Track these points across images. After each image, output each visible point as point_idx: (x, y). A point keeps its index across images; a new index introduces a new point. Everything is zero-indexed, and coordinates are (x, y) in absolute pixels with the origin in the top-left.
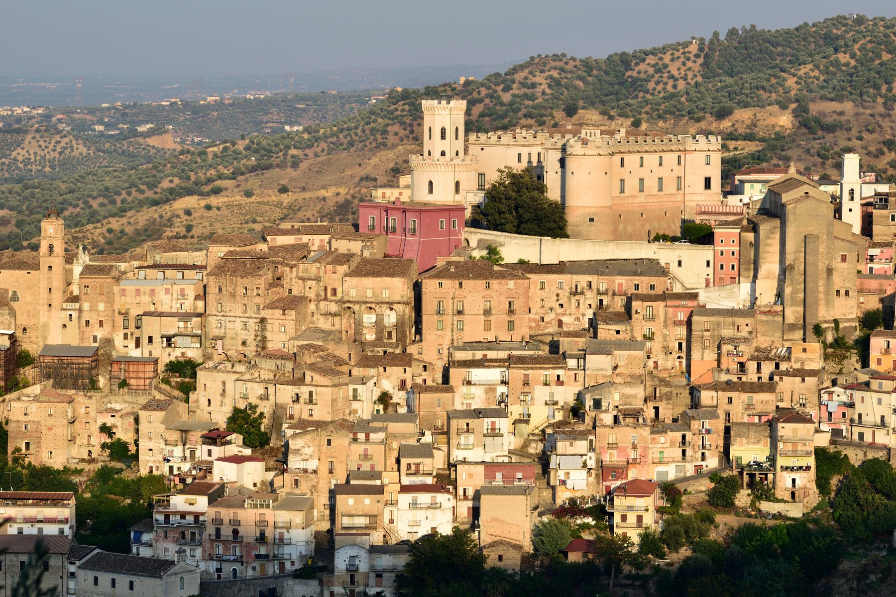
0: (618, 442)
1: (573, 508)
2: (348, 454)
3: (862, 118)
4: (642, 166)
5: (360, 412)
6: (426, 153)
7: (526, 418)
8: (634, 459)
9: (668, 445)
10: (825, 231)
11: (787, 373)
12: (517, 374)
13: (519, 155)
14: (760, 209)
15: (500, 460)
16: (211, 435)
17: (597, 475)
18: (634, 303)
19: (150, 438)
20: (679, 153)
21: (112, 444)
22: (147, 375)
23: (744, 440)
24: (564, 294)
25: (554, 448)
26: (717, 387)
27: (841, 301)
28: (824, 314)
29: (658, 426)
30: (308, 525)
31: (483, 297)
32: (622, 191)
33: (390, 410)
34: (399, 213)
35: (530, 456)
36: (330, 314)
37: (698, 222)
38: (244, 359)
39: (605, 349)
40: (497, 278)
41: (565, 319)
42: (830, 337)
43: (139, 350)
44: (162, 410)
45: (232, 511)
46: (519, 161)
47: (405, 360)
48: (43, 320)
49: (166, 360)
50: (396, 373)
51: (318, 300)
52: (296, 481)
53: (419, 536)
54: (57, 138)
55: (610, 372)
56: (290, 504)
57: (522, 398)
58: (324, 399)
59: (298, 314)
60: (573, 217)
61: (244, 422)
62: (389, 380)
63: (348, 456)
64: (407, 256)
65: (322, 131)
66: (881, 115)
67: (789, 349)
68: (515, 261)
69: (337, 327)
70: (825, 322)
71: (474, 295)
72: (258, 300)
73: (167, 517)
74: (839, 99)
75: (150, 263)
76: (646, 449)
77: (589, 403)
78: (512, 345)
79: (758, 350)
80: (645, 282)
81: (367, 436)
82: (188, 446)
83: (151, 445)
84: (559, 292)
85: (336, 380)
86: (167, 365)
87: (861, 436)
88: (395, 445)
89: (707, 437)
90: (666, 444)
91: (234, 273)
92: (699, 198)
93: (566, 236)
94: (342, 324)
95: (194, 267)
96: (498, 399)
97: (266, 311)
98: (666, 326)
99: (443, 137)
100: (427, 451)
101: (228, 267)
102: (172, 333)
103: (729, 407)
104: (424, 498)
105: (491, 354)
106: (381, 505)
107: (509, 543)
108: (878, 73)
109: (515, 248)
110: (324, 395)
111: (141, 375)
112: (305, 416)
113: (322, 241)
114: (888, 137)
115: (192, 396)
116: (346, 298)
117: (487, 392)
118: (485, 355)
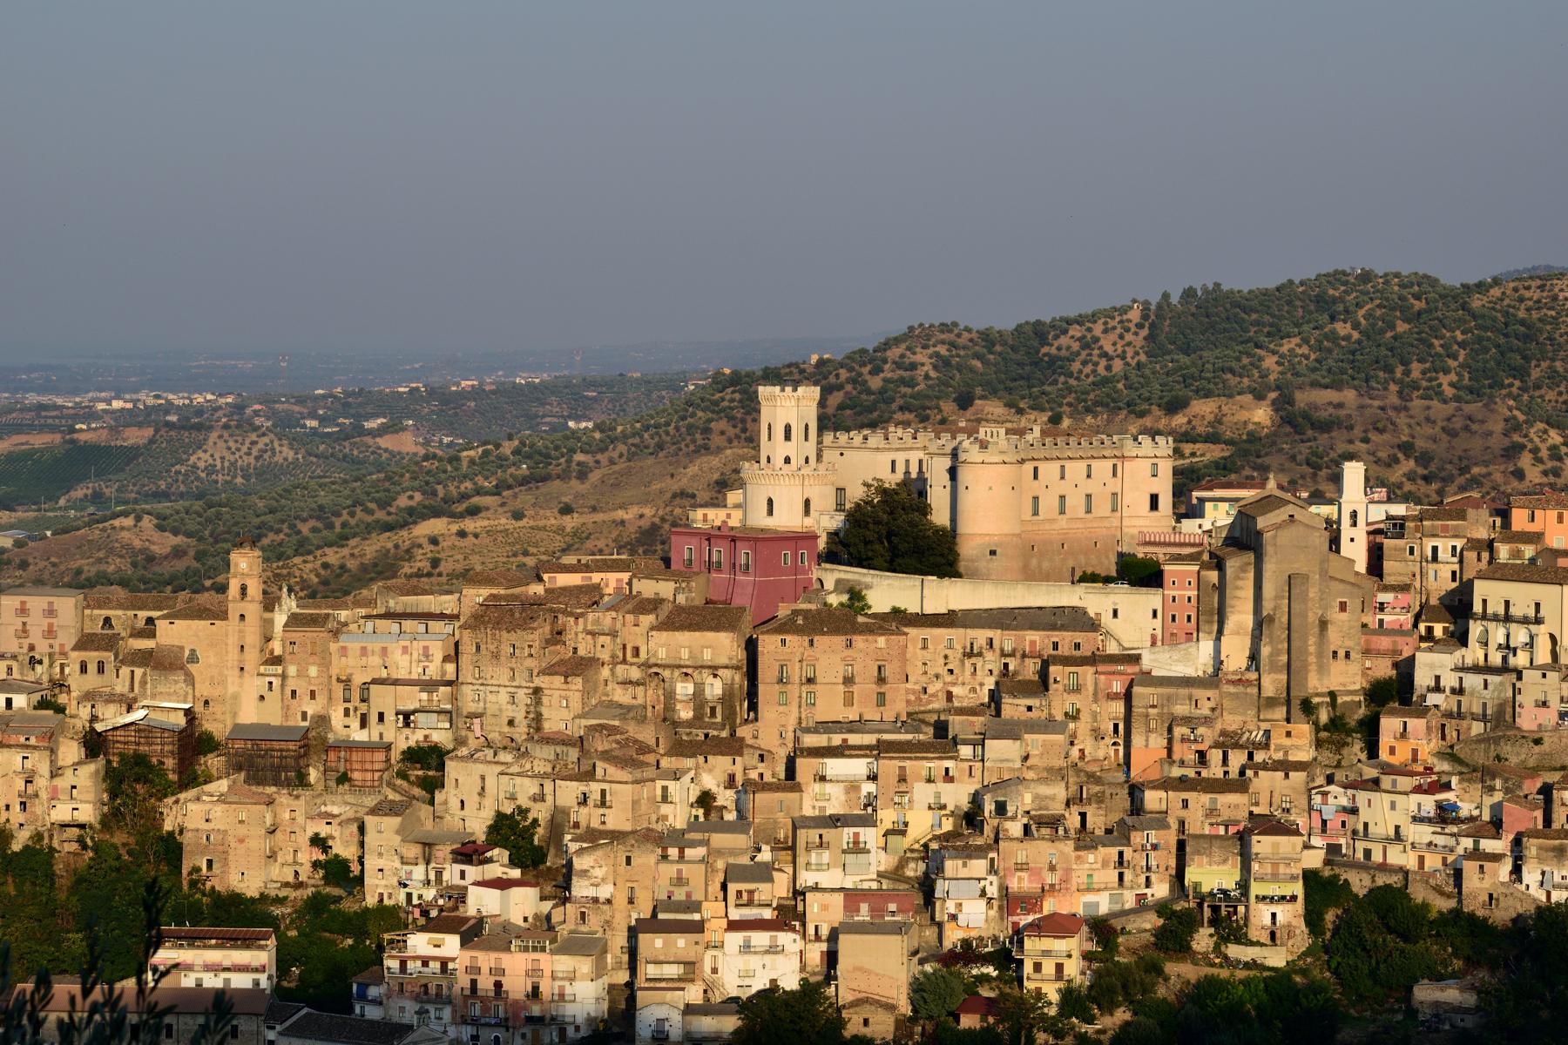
0: (1030, 861)
1: (967, 953)
2: (655, 877)
3: (1368, 412)
4: (1062, 478)
5: (671, 818)
6: (763, 460)
7: (901, 827)
8: (1052, 886)
9: (1099, 866)
10: (1317, 569)
11: (1264, 766)
12: (889, 767)
13: (893, 462)
14: (1226, 539)
15: (866, 886)
16: (464, 851)
17: (1000, 908)
18: (1052, 669)
19: (380, 854)
20: (1115, 461)
21: (327, 862)
22: (377, 766)
23: (1205, 859)
24: (955, 656)
25: (940, 869)
26: (1166, 784)
27: (1338, 667)
28: (1315, 684)
29: (1085, 839)
30: (599, 976)
31: (843, 660)
32: (1036, 513)
33: (714, 816)
34: (727, 543)
35: (907, 880)
36: (631, 682)
37: (1140, 556)
38: (511, 745)
39: (1012, 732)
40: (861, 633)
41: (956, 690)
42: (1324, 717)
43: (365, 732)
44: (397, 815)
45: (493, 955)
46: (893, 470)
47: (733, 746)
48: (231, 689)
49: (403, 746)
50: (722, 764)
51: (614, 662)
52: (583, 914)
53: (754, 990)
54: (254, 437)
55: (1018, 765)
56: (575, 946)
57: (897, 799)
58: (621, 801)
59: (585, 682)
60: (968, 549)
61: (510, 831)
62: (712, 775)
64: (737, 601)
65: (620, 429)
66: (1395, 408)
67: (1267, 733)
68: (887, 610)
69: (640, 701)
70: (1318, 695)
71: (830, 656)
72: (530, 663)
73: (403, 964)
74: (1336, 385)
75: (382, 611)
76: (1068, 871)
77: (989, 807)
78: (883, 727)
79: (1223, 733)
80: (1066, 639)
81: (682, 852)
82: (433, 865)
83: (381, 863)
84: (948, 652)
85: (638, 775)
86: (403, 753)
87: (1368, 853)
88: (720, 864)
89: (1152, 854)
90: (1097, 864)
91: (497, 625)
92: (1141, 522)
93: (959, 576)
94: (647, 696)
95: (441, 616)
96: (863, 801)
97: (542, 678)
98: (1096, 700)
99: (788, 437)
100: (764, 873)
101: (490, 618)
102: (412, 708)
103: (1183, 813)
104: (760, 938)
105: (854, 739)
106: (700, 948)
107: (878, 1002)
108: (1391, 350)
109: (888, 591)
110: (622, 794)
111: (368, 766)
112: (595, 824)
113: (618, 581)
114: (1404, 439)
115: (439, 797)
116: (652, 661)
117: (847, 791)
118: (845, 741)
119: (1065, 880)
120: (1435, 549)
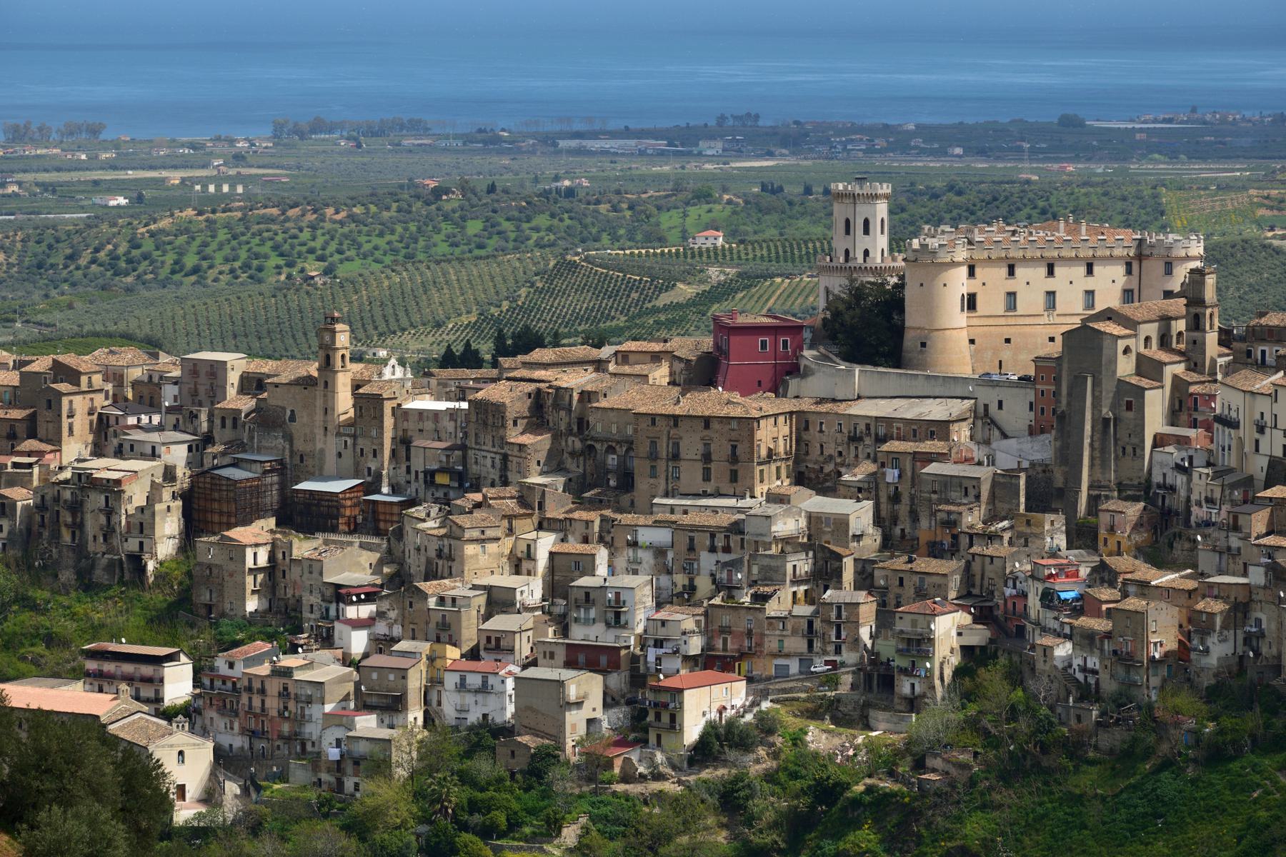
9: (789, 633)
48: (319, 446)
63: (427, 623)
73: (212, 682)
76: (763, 635)
93: (898, 364)
102: (435, 467)
117: (656, 558)
119: (760, 644)
120: (1263, 352)
